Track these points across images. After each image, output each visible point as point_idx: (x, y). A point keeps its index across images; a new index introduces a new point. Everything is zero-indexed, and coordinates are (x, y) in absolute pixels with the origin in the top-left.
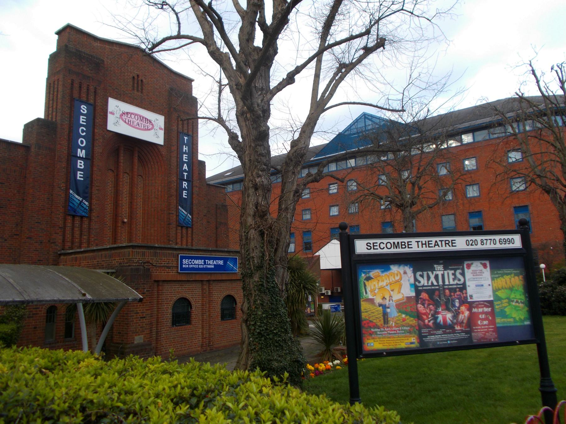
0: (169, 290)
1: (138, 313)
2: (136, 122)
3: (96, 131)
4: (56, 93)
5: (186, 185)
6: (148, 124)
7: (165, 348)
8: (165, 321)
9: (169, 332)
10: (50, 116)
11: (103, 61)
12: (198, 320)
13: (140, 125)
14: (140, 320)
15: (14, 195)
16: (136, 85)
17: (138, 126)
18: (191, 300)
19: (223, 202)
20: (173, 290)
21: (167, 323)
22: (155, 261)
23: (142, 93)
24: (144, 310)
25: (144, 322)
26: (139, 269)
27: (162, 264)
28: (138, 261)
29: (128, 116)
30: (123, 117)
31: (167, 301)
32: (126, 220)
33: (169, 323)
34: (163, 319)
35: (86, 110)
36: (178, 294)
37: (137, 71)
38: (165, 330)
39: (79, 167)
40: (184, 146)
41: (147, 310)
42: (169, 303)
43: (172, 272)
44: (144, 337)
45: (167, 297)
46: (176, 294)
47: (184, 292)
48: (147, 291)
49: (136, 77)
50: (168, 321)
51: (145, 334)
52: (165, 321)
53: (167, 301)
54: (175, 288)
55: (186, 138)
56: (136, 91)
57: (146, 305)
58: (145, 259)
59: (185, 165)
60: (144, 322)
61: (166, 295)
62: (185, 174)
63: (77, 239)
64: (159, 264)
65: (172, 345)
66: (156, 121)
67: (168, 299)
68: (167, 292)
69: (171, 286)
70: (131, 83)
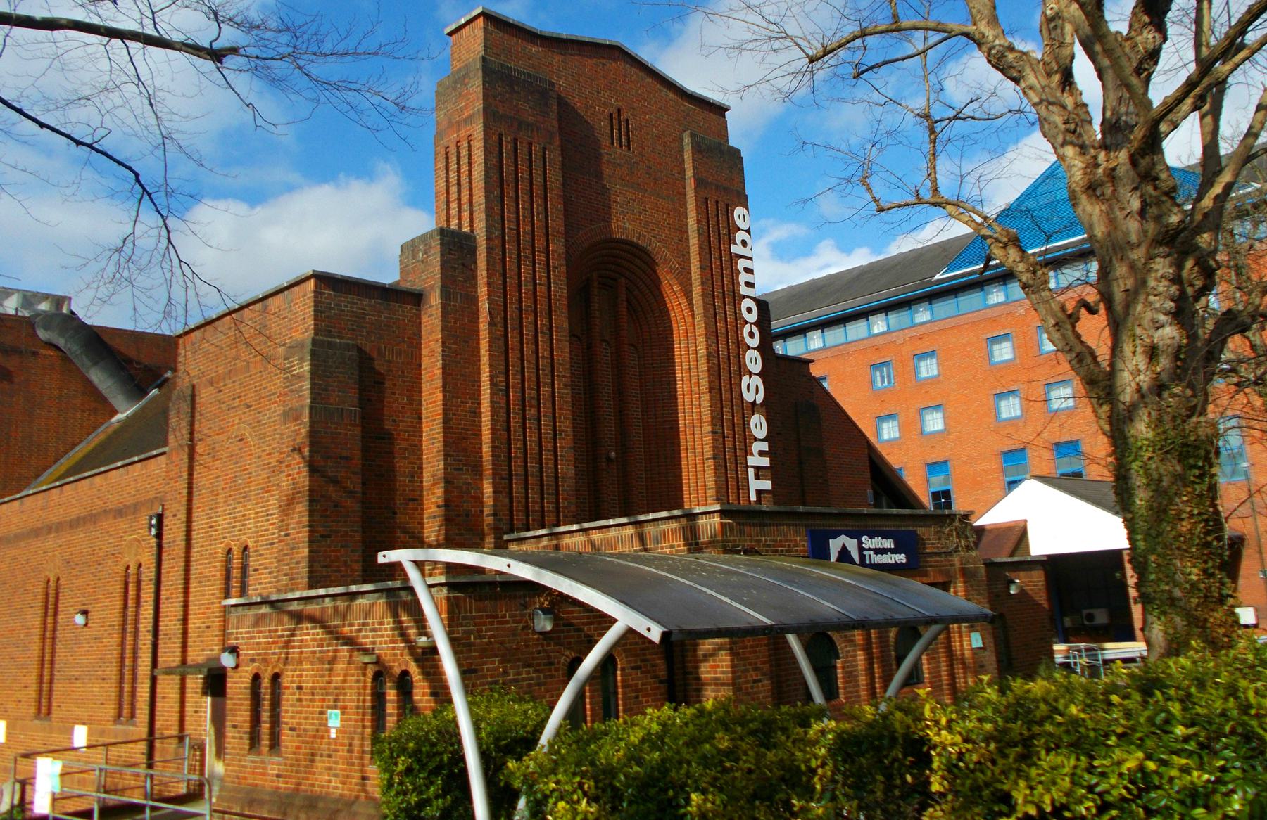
4: (465, 168)
10: (454, 222)
11: (552, 84)
15: (403, 408)
23: (629, 149)
32: (613, 454)
37: (617, 100)
60: (760, 692)
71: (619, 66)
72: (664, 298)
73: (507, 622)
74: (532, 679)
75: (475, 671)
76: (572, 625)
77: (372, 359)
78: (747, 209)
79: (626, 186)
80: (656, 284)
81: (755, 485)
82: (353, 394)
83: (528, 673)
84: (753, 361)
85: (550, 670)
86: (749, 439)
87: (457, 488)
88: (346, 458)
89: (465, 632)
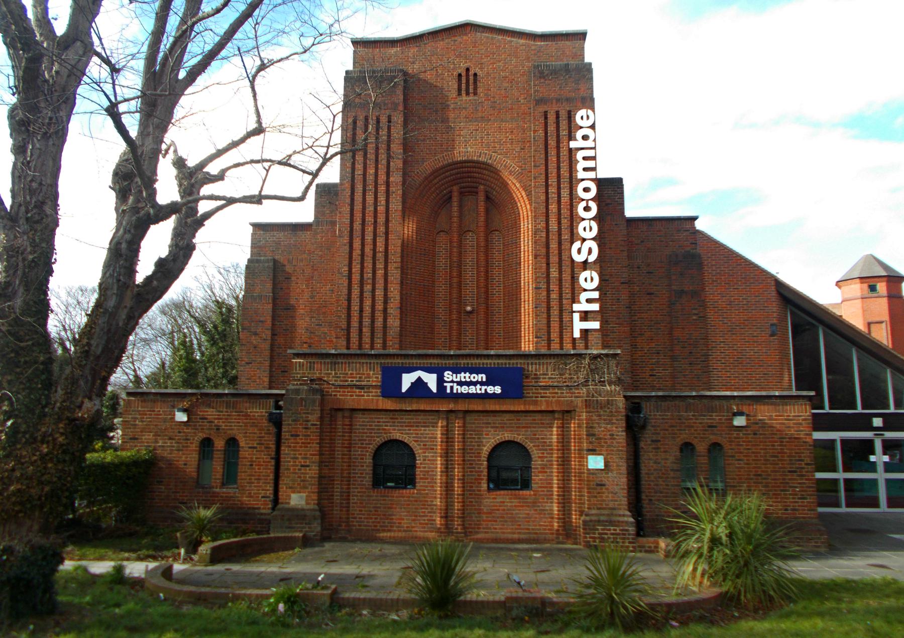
0: (366, 426)
1: (297, 458)
3: (391, 179)
7: (357, 522)
8: (359, 477)
9: (368, 496)
12: (428, 483)
14: (299, 470)
18: (413, 444)
19: (688, 249)
20: (376, 426)
21: (362, 481)
22: (333, 377)
23: (475, 94)
24: (306, 454)
25: (308, 474)
26: (299, 389)
27: (347, 381)
28: (301, 377)
31: (362, 444)
33: (368, 479)
34: (354, 473)
36: (385, 433)
37: (466, 62)
38: (359, 492)
41: (311, 455)
42: (366, 448)
43: (369, 396)
44: (307, 496)
45: (362, 436)
46: (381, 433)
47: (399, 430)
48: (313, 425)
49: (464, 74)
50: (366, 478)
51: (309, 492)
52: (359, 477)
53: (362, 444)
54: (378, 422)
56: (465, 95)
57: (311, 447)
58: (316, 373)
60: (308, 474)
61: (359, 433)
63: (367, 343)
64: (341, 381)
65: (371, 518)
67: (365, 440)
68: (364, 429)
69: (371, 418)
70: (456, 86)
71: (468, 37)
72: (512, 194)
73: (160, 415)
74: (173, 447)
75: (137, 439)
76: (206, 419)
77: (285, 266)
78: (593, 109)
79: (470, 121)
80: (505, 185)
81: (578, 326)
82: (269, 286)
83: (171, 443)
84: (588, 229)
85: (187, 443)
86: (575, 292)
87: (317, 336)
88: (262, 321)
89: (132, 418)
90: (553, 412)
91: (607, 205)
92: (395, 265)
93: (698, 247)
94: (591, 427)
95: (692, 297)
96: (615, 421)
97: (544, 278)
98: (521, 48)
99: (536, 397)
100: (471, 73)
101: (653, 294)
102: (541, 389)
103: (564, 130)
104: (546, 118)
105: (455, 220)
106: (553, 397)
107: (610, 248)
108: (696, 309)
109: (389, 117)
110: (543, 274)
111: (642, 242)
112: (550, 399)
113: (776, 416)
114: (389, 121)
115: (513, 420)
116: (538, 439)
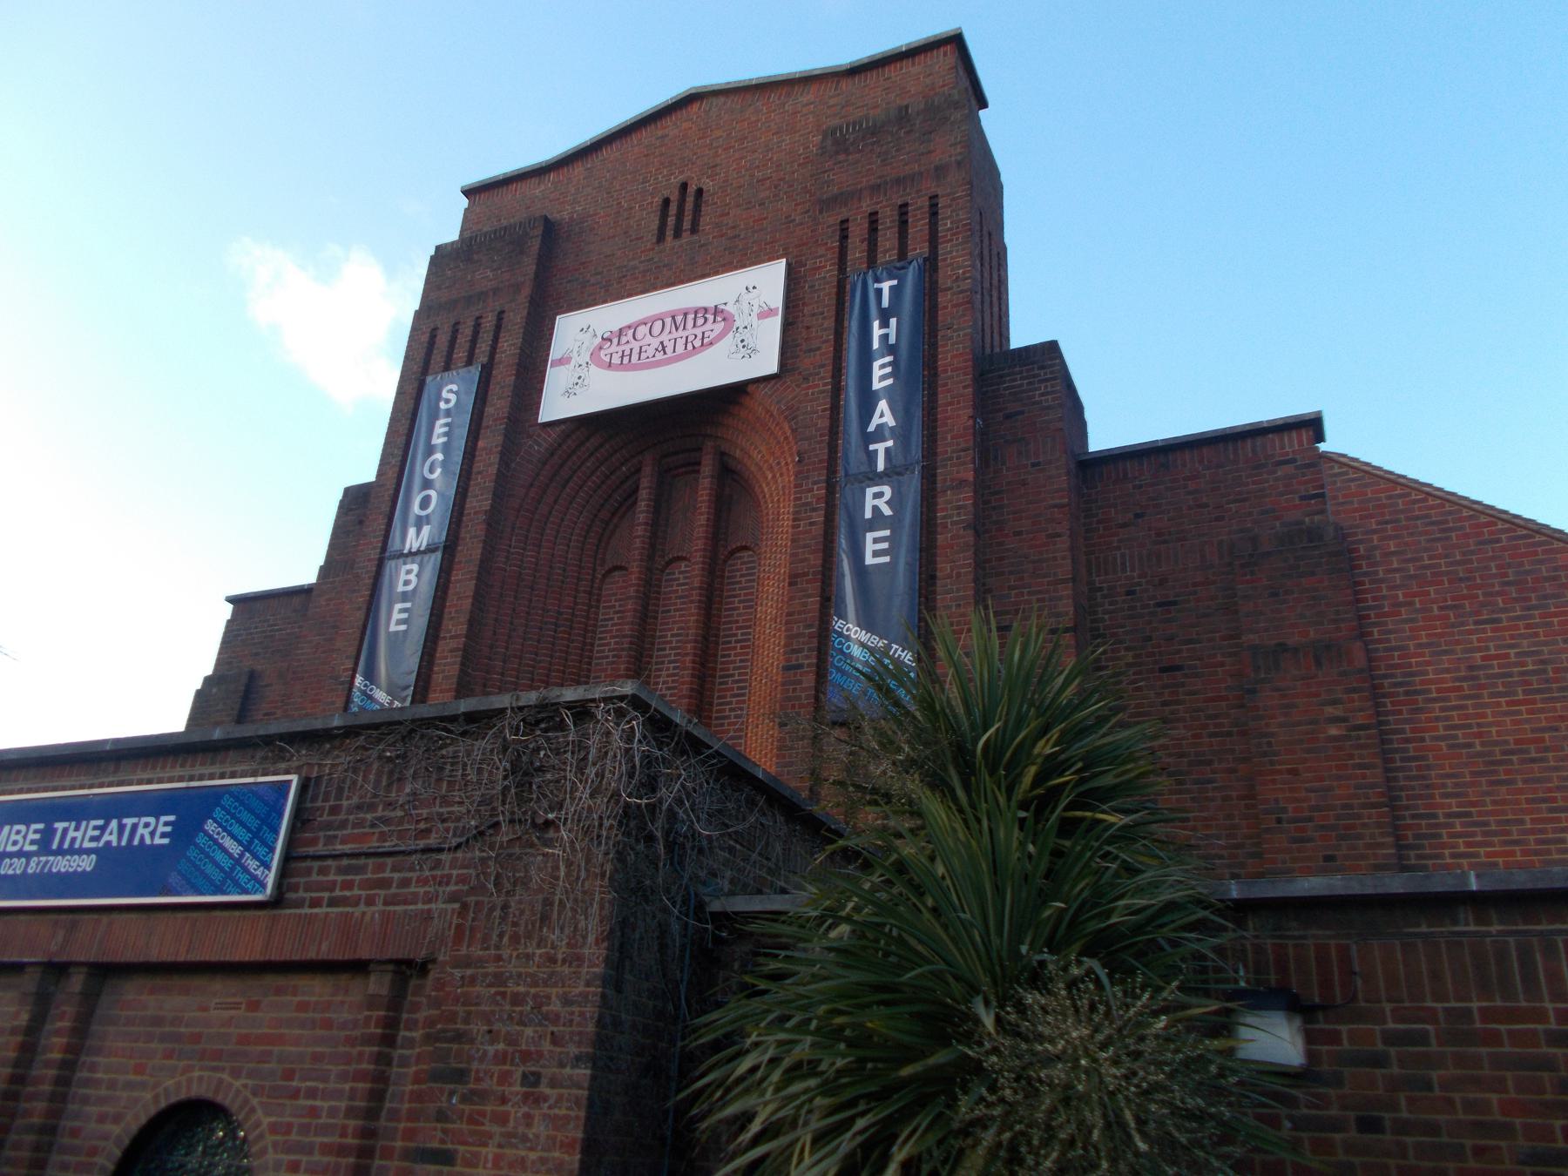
2: (655, 343)
3: (481, 444)
5: (882, 504)
6: (709, 326)
13: (669, 350)
16: (671, 221)
17: (659, 356)
29: (624, 340)
30: (602, 353)
35: (453, 398)
37: (681, 173)
39: (400, 588)
40: (876, 324)
49: (674, 197)
55: (886, 286)
59: (883, 405)
62: (880, 448)
66: (746, 297)
90: (358, 967)
91: (1008, 417)
92: (453, 644)
93: (1330, 507)
94: (459, 1037)
95: (1319, 664)
96: (556, 1006)
97: (811, 636)
98: (805, 110)
99: (315, 903)
100: (692, 189)
101: (1179, 668)
102: (341, 871)
103: (886, 251)
104: (844, 237)
105: (640, 530)
106: (370, 901)
107: (1019, 533)
108: (1334, 702)
109: (500, 316)
110: (810, 626)
111: (1137, 516)
112: (362, 908)
113: (1486, 1014)
114: (498, 327)
115: (236, 1006)
116: (295, 1094)
